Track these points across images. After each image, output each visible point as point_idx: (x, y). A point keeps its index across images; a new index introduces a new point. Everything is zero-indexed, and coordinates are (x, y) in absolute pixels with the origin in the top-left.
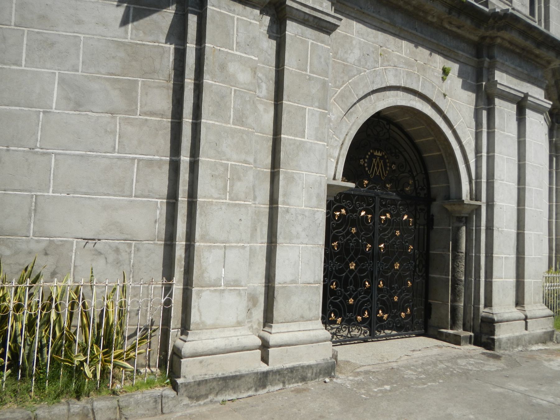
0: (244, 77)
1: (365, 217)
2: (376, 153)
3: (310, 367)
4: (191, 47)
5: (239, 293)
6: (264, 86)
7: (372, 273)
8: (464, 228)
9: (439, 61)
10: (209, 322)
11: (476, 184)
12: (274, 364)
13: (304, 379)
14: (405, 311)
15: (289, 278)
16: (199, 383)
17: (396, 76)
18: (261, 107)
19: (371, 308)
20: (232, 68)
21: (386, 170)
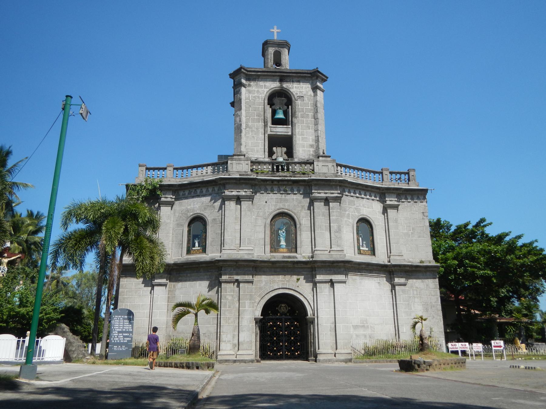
0: (230, 298)
1: (279, 324)
2: (283, 305)
3: (247, 360)
4: (220, 294)
5: (230, 344)
6: (236, 298)
7: (282, 340)
8: (312, 325)
9: (295, 277)
10: (224, 349)
11: (313, 311)
12: (237, 359)
13: (245, 362)
14: (298, 352)
15: (242, 340)
16: (221, 360)
17: (278, 286)
18: (235, 303)
19: (283, 351)
20: (227, 297)
21: (287, 309)
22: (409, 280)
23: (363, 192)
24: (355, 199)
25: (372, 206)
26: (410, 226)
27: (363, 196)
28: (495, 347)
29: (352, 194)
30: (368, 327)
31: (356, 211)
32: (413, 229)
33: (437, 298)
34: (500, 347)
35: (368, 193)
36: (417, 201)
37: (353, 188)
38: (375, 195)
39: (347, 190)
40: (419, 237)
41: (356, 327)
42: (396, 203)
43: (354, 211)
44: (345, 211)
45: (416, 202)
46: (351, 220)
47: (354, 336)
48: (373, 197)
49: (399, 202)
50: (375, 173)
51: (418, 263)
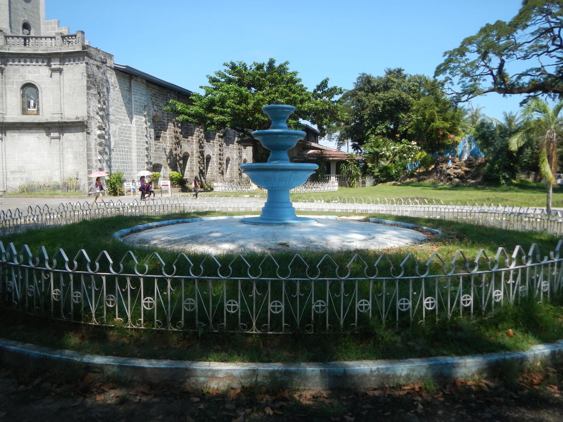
22: (65, 134)
23: (28, 60)
24: (21, 67)
25: (39, 71)
26: (71, 87)
27: (28, 63)
28: (163, 185)
29: (16, 63)
30: (25, 172)
31: (20, 78)
32: (74, 89)
33: (84, 148)
34: (167, 185)
35: (34, 60)
36: (77, 62)
37: (17, 57)
38: (43, 60)
39: (11, 60)
40: (78, 96)
41: (13, 172)
42: (59, 66)
43: (19, 77)
44: (10, 78)
45: (77, 64)
46: (15, 86)
47: (11, 179)
48: (40, 63)
49: (63, 65)
50: (51, 38)
51: (75, 119)
